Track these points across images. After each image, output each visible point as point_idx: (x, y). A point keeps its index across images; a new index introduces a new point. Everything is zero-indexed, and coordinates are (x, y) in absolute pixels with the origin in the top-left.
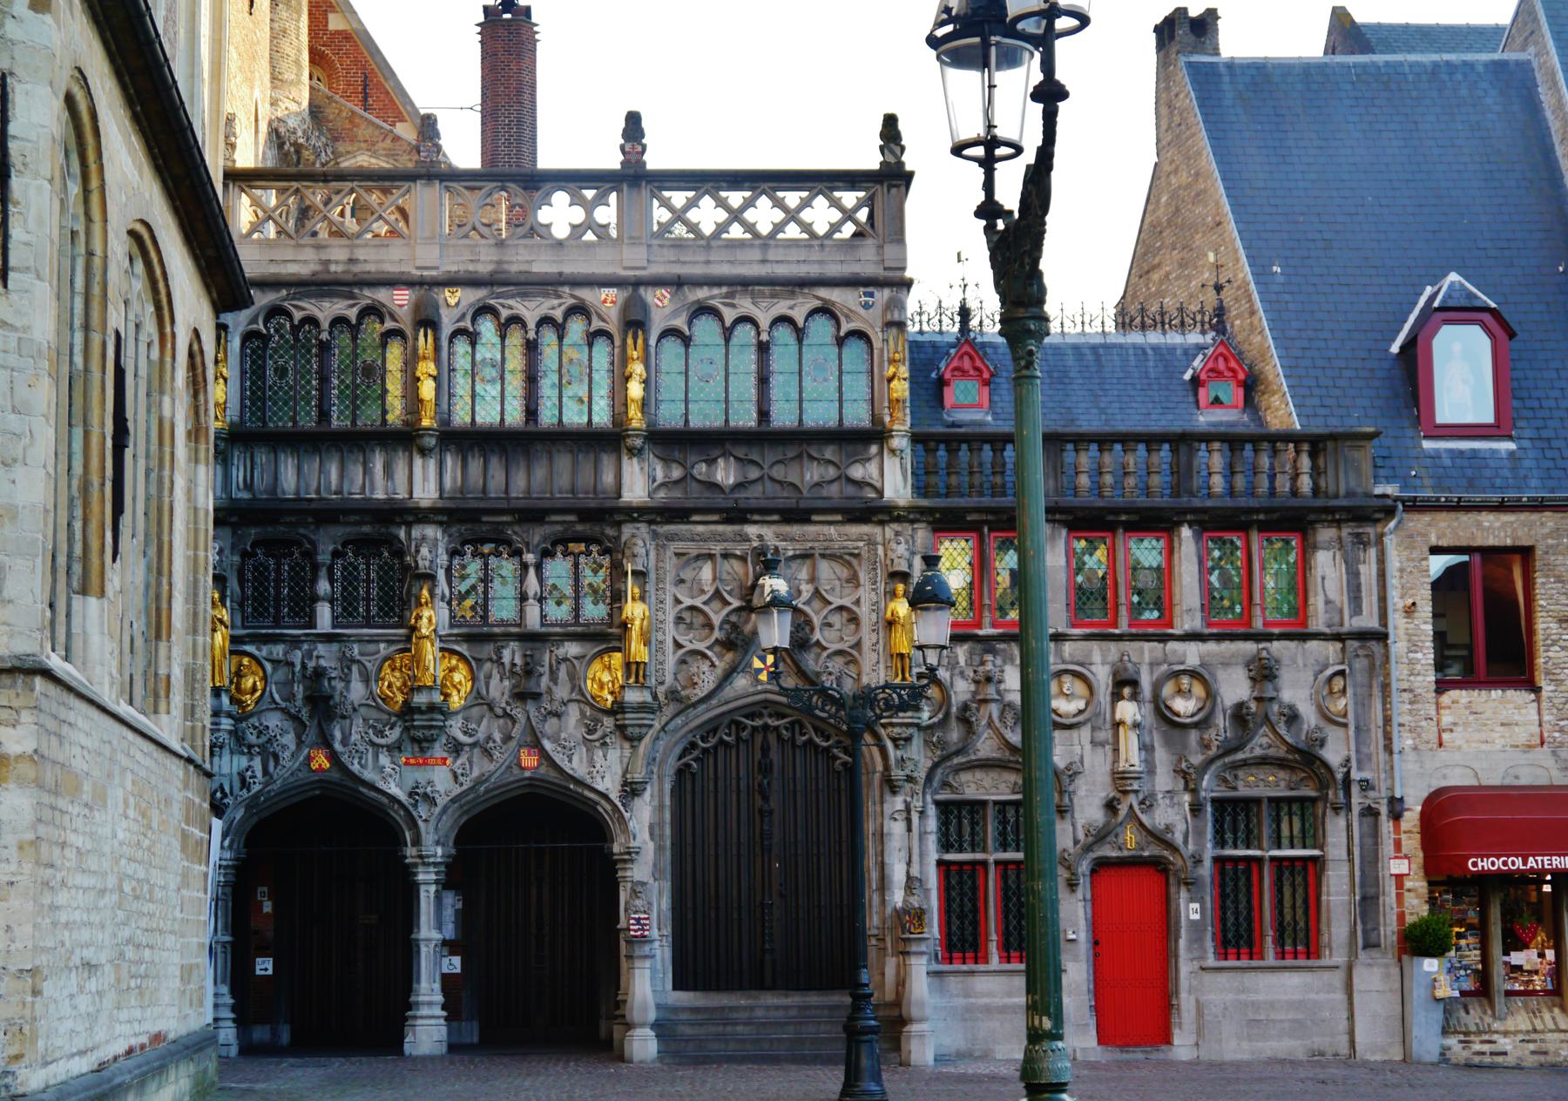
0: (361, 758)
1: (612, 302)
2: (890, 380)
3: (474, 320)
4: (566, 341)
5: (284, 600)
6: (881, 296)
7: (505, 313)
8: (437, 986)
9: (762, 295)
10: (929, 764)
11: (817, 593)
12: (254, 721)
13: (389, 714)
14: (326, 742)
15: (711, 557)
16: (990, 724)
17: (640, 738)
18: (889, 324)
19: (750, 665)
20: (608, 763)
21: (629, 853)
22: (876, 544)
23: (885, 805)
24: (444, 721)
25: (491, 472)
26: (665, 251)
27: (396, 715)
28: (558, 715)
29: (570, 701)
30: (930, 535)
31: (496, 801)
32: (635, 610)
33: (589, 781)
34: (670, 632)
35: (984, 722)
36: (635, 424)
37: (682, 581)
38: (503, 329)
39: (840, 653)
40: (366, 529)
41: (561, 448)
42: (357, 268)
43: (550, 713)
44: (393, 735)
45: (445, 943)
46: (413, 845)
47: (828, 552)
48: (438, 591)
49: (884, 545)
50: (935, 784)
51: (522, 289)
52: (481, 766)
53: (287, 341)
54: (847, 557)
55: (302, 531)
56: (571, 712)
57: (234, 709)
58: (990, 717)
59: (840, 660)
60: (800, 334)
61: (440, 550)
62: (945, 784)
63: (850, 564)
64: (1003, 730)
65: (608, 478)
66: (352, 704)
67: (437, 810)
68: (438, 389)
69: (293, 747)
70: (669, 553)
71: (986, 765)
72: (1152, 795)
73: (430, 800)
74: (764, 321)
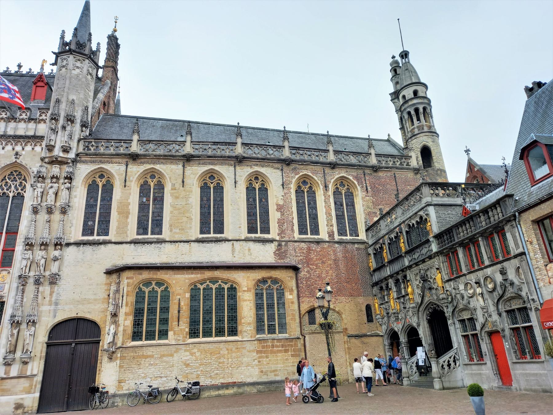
10: (452, 310)
57: (381, 317)
72: (491, 312)
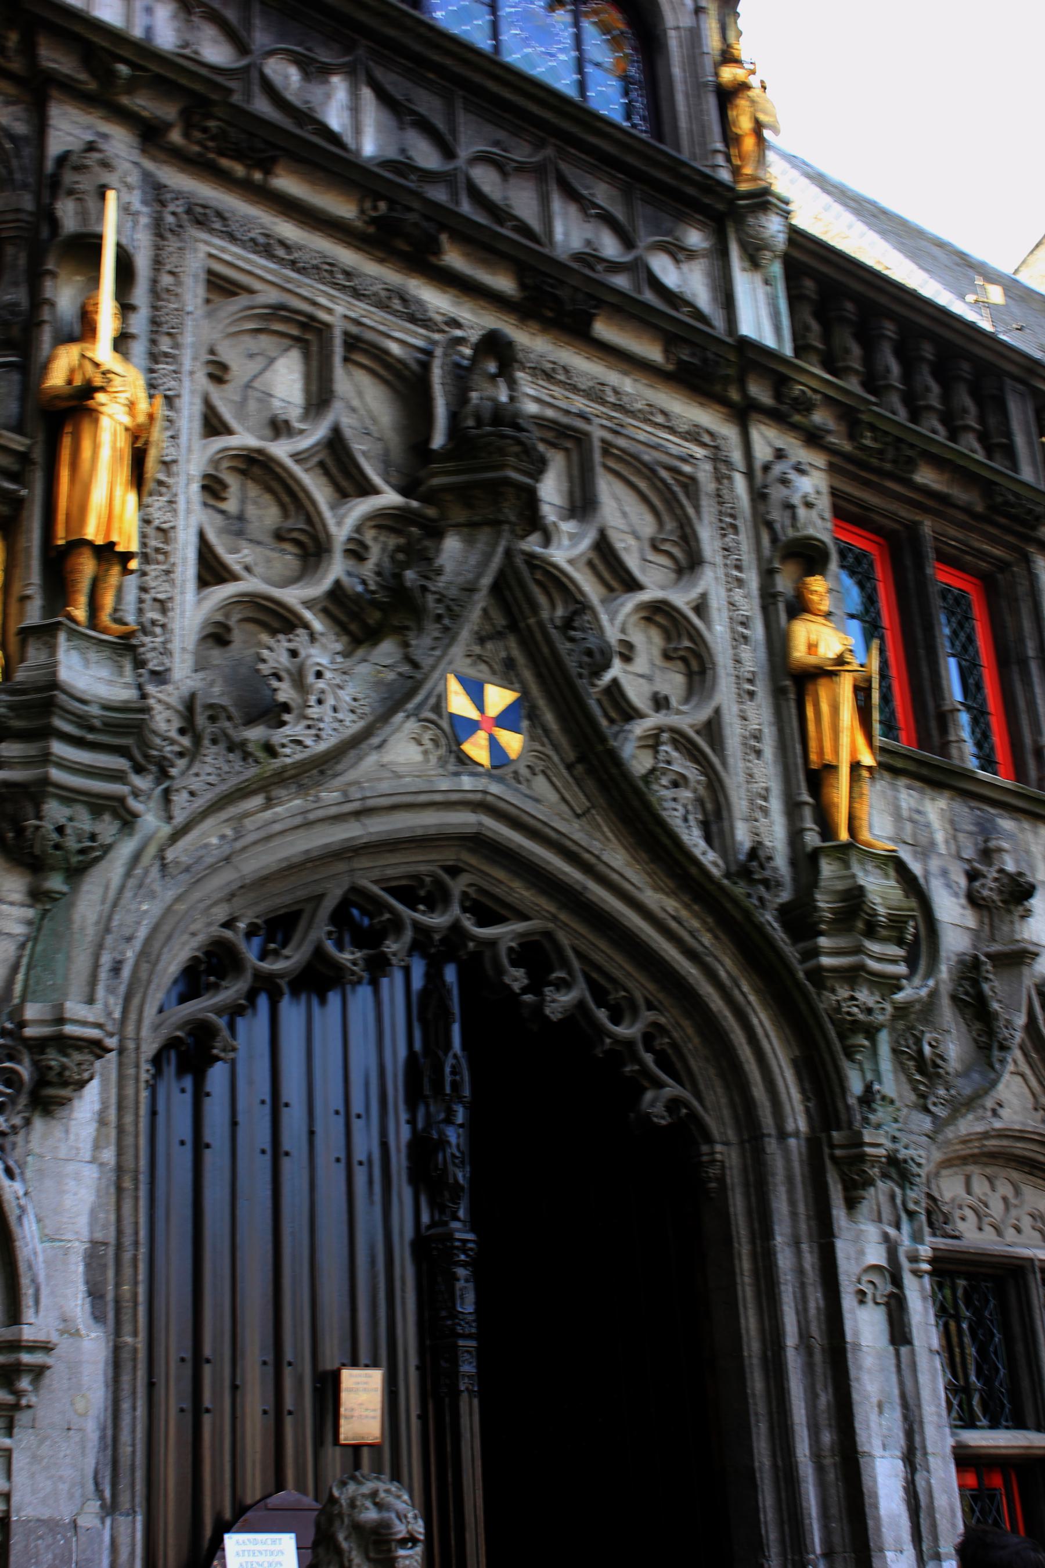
47: (621, 442)
49: (749, 474)
54: (664, 474)
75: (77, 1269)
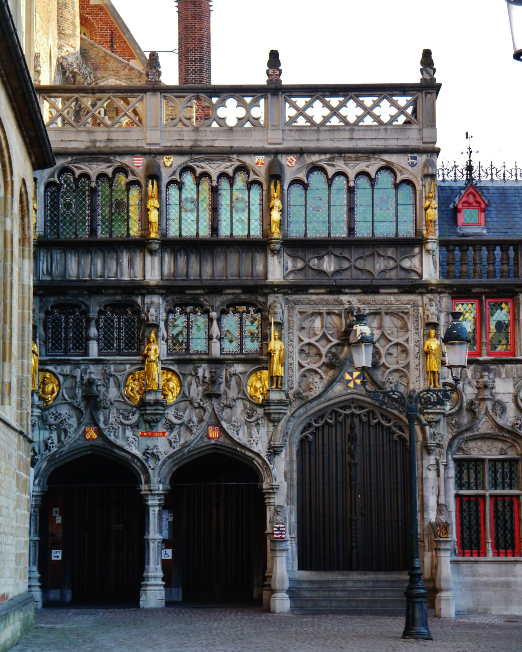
0: (115, 432)
1: (262, 164)
2: (426, 209)
3: (181, 175)
4: (235, 187)
5: (70, 339)
6: (422, 159)
7: (199, 171)
8: (159, 567)
9: (350, 159)
10: (450, 436)
11: (383, 335)
12: (53, 410)
13: (132, 406)
14: (95, 423)
15: (320, 314)
16: (487, 413)
17: (279, 421)
18: (426, 176)
19: (343, 377)
20: (260, 435)
21: (272, 489)
22: (418, 306)
23: (424, 461)
24: (165, 410)
25: (191, 264)
26: (293, 133)
27: (136, 407)
28: (230, 407)
29: (238, 399)
30: (450, 301)
31: (194, 457)
32: (275, 345)
33: (248, 446)
34: (296, 358)
35: (483, 412)
36: (276, 236)
37: (303, 328)
38: (198, 180)
39: (397, 370)
40: (118, 298)
41: (232, 250)
42: (112, 145)
43: (226, 406)
44: (134, 419)
45: (164, 541)
46: (146, 483)
47: (390, 311)
48: (160, 334)
49: (423, 307)
50: (454, 449)
51: (209, 156)
52: (185, 437)
53: (71, 188)
54: (401, 314)
55: (80, 299)
56: (238, 405)
57: (41, 403)
58: (487, 409)
59: (396, 375)
60: (373, 182)
61: (161, 311)
62: (460, 449)
63: (402, 318)
64: (494, 417)
65: (260, 268)
66: (110, 400)
67: (160, 463)
68: (160, 216)
69: (75, 426)
70: (296, 312)
71: (484, 437)
73: (156, 457)
74: (352, 175)
75: (283, 475)
